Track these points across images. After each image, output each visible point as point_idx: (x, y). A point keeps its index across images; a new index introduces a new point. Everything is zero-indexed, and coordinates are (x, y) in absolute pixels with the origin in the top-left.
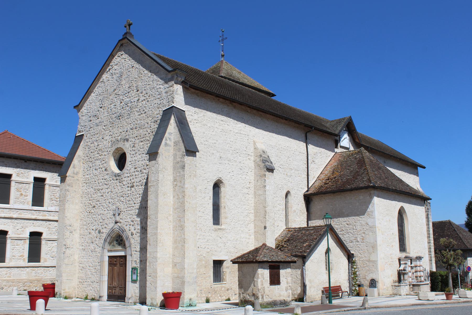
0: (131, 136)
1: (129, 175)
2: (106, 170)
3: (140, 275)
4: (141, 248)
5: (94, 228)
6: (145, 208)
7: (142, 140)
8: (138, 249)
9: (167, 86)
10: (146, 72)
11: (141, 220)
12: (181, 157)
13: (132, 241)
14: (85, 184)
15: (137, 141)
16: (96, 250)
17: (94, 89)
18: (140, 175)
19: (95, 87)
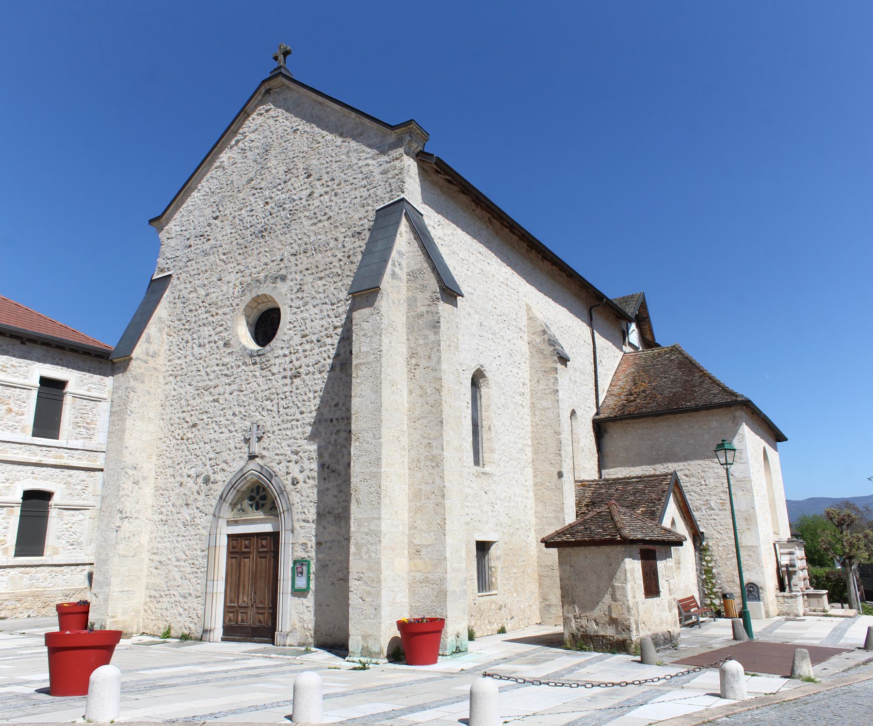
0: (294, 268)
1: (287, 352)
2: (225, 345)
3: (317, 578)
4: (319, 514)
5: (192, 472)
7: (323, 274)
8: (312, 514)
9: (385, 158)
10: (329, 137)
11: (319, 448)
12: (427, 303)
13: (295, 498)
14: (171, 379)
15: (309, 279)
16: (197, 521)
17: (199, 182)
18: (317, 351)
19: (202, 178)
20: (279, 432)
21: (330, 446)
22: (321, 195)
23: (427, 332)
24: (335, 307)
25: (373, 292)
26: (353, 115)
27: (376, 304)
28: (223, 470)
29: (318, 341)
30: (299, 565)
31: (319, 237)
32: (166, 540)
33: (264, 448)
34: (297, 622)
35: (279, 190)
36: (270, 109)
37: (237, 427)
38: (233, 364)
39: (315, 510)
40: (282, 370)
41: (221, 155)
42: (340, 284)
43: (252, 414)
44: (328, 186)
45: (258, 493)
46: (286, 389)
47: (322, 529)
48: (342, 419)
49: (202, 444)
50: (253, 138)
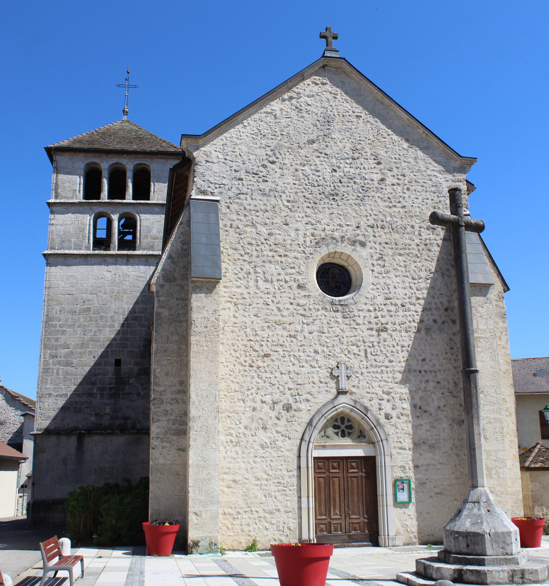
0: (372, 238)
2: (299, 287)
3: (416, 492)
4: (414, 444)
6: (409, 371)
7: (402, 252)
8: (408, 443)
10: (395, 137)
13: (390, 429)
15: (390, 252)
16: (279, 443)
18: (401, 313)
19: (250, 116)
20: (368, 374)
21: (420, 391)
22: (393, 185)
23: (497, 319)
24: (416, 281)
25: (486, 287)
26: (421, 130)
27: (488, 295)
28: (308, 401)
29: (403, 306)
30: (398, 484)
31: (395, 219)
33: (354, 386)
34: (400, 527)
35: (347, 163)
36: (326, 84)
37: (320, 363)
38: (311, 307)
39: (411, 441)
40: (366, 322)
41: (272, 103)
43: (337, 355)
44: (398, 179)
45: (343, 423)
46: (372, 339)
47: (418, 455)
48: (430, 372)
49: (278, 375)
50: (310, 103)
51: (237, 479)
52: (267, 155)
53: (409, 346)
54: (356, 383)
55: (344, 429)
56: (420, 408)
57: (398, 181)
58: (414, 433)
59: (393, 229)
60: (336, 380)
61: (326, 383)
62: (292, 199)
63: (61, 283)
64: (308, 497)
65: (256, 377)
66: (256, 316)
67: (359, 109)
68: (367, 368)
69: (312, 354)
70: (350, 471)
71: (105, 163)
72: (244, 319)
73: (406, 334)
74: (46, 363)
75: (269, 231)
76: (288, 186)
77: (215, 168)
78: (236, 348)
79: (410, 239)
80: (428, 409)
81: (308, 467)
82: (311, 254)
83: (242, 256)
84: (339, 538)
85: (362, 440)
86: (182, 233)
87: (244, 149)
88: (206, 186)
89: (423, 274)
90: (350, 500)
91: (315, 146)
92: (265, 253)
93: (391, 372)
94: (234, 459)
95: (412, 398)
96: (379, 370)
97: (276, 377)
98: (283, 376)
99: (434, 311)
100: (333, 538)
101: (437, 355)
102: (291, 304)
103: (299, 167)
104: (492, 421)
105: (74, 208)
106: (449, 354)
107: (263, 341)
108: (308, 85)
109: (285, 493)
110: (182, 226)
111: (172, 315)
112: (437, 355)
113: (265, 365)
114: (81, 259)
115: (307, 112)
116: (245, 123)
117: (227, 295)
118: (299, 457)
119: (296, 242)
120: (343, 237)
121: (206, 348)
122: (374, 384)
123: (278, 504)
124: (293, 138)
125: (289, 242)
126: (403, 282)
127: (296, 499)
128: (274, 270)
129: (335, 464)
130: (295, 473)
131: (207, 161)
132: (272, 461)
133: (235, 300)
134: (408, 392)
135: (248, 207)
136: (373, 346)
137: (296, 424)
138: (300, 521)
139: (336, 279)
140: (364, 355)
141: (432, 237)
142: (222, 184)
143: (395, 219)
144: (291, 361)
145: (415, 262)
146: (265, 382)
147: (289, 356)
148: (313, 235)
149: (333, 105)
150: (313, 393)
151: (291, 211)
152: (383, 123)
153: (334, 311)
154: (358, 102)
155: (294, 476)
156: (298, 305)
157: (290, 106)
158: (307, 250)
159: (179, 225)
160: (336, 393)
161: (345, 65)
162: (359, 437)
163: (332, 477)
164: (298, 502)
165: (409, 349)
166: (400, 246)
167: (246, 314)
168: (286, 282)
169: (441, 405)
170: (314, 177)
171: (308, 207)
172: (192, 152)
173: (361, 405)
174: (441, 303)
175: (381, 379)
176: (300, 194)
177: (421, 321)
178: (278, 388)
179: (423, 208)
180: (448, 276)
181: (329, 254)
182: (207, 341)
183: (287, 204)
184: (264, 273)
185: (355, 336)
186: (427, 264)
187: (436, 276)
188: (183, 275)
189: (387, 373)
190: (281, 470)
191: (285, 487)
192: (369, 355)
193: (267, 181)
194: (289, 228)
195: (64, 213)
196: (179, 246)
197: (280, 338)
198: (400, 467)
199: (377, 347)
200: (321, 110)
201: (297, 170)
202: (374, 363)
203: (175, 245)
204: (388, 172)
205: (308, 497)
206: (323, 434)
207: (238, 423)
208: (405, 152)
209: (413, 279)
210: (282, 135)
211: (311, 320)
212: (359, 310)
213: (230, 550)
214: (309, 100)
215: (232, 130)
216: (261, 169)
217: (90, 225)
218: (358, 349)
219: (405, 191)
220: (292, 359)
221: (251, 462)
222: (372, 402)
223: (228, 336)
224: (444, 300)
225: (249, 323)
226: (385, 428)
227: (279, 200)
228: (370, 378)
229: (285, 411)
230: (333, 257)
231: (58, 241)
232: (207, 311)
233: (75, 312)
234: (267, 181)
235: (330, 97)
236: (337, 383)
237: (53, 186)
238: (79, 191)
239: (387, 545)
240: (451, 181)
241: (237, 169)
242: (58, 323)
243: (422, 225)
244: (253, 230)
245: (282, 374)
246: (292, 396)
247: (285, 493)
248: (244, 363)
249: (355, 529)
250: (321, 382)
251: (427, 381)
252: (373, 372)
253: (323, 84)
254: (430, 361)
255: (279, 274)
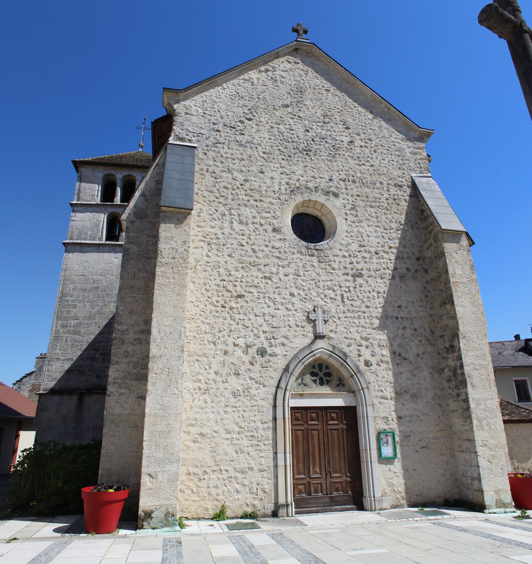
0: (344, 190)
1: (346, 254)
3: (401, 446)
4: (396, 393)
5: (241, 342)
7: (373, 204)
8: (389, 392)
10: (360, 109)
15: (362, 204)
16: (253, 391)
18: (375, 260)
20: (346, 319)
22: (361, 147)
24: (388, 232)
28: (283, 345)
29: (377, 253)
32: (208, 410)
33: (331, 331)
34: (386, 487)
35: (318, 126)
36: (298, 63)
37: (296, 306)
38: (286, 250)
39: (392, 389)
41: (250, 72)
42: (390, 216)
43: (313, 298)
45: (321, 370)
46: (348, 284)
47: (401, 406)
48: (407, 319)
49: (252, 316)
50: (284, 76)
51: (204, 432)
52: (244, 113)
53: (384, 293)
54: (333, 328)
55: (322, 376)
56: (400, 355)
57: (366, 144)
58: (395, 382)
59: (363, 184)
60: (312, 324)
61: (302, 327)
62: (267, 151)
63: (76, 266)
64: (285, 453)
65: (228, 318)
66: (230, 256)
67: (328, 85)
68: (344, 312)
69: (288, 297)
70: (330, 423)
71: (119, 174)
72: (218, 258)
73: (381, 281)
74: (57, 332)
75: (245, 178)
76: (264, 140)
77: (194, 119)
78: (207, 287)
79: (380, 193)
80: (407, 356)
81: (284, 418)
82: (286, 201)
83: (217, 198)
84: (320, 501)
85: (341, 389)
86: (157, 174)
87: (223, 106)
88: (184, 133)
89: (394, 225)
90: (331, 456)
91: (289, 109)
92: (241, 197)
93: (368, 318)
94: (202, 408)
95: (391, 345)
96: (356, 315)
97: (250, 319)
98: (258, 318)
99: (406, 260)
100: (313, 501)
101: (413, 302)
102: (267, 246)
103: (274, 125)
104: (478, 367)
105: (91, 209)
106: (424, 302)
107: (237, 281)
108: (283, 62)
109: (258, 448)
110: (157, 167)
111: (141, 251)
112: (413, 302)
113: (239, 306)
114: (94, 248)
115: (282, 82)
116: (225, 85)
117: (200, 234)
118: (275, 406)
119: (272, 189)
120: (316, 188)
121: (172, 280)
122: (352, 330)
123: (251, 461)
124: (269, 102)
125: (264, 188)
126: (376, 231)
127: (271, 455)
128: (249, 213)
129: (313, 415)
130: (271, 425)
131: (186, 113)
132: (244, 411)
133: (208, 240)
134: (386, 338)
135: (225, 155)
136: (350, 291)
137: (271, 369)
138: (276, 481)
139: (310, 228)
140: (341, 300)
141: (400, 193)
142: (200, 133)
143: (365, 176)
144: (266, 303)
145: (385, 214)
146: (238, 324)
147: (264, 297)
148: (288, 184)
149: (305, 79)
150: (289, 337)
151: (267, 161)
152: (349, 97)
153: (310, 255)
154: (327, 79)
155: (269, 428)
156: (273, 247)
157: (266, 76)
158: (283, 197)
159: (155, 166)
160: (313, 338)
161: (315, 49)
162: (338, 385)
163: (311, 430)
164: (274, 459)
165: (385, 295)
166: (371, 199)
167: (220, 254)
168: (261, 225)
169: (420, 351)
170: (288, 134)
171: (283, 159)
172: (172, 104)
173: (340, 351)
174: (413, 253)
175: (359, 324)
176: (275, 148)
177: (395, 269)
178: (252, 331)
179: (390, 167)
180: (417, 228)
181: (304, 202)
182: (174, 273)
183: (262, 155)
184: (239, 216)
185: (331, 280)
186: (396, 216)
187: (407, 228)
188: (155, 212)
189: (365, 318)
190: (255, 421)
191: (259, 441)
192: (346, 300)
193: (243, 134)
194: (265, 176)
195: (83, 212)
196: (154, 185)
197: (254, 279)
198: (383, 418)
199: (353, 292)
200: (294, 82)
201: (272, 128)
202: (351, 308)
203: (149, 183)
204: (356, 136)
205: (285, 453)
206: (300, 382)
207: (207, 367)
208: (370, 122)
209: (385, 229)
210: (258, 98)
211: (286, 262)
212: (334, 256)
213: (193, 519)
214: (283, 74)
215: (212, 90)
216: (239, 124)
217: (104, 222)
218: (334, 293)
219: (373, 152)
220: (267, 301)
221: (222, 413)
222: (351, 348)
223: (200, 275)
224: (415, 250)
225: (222, 263)
226: (365, 376)
227: (254, 151)
228: (348, 323)
229: (259, 356)
230: (308, 207)
231: (76, 233)
232: (176, 242)
233: (86, 290)
234: (243, 134)
235: (302, 73)
236: (314, 327)
237: (76, 192)
238: (97, 196)
239: (374, 508)
240: (413, 148)
241: (215, 122)
242: (71, 299)
243: (390, 182)
244: (229, 175)
245: (256, 316)
246: (267, 340)
247: (258, 448)
248: (215, 303)
249: (337, 490)
250: (297, 326)
251: (404, 328)
252: (350, 317)
253: (295, 63)
254: (406, 308)
255: (255, 217)
